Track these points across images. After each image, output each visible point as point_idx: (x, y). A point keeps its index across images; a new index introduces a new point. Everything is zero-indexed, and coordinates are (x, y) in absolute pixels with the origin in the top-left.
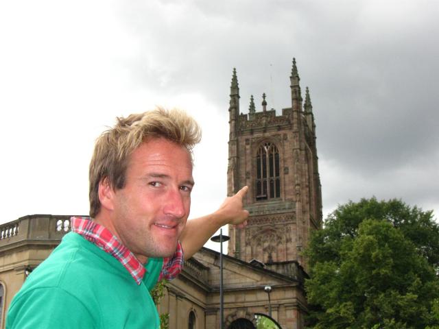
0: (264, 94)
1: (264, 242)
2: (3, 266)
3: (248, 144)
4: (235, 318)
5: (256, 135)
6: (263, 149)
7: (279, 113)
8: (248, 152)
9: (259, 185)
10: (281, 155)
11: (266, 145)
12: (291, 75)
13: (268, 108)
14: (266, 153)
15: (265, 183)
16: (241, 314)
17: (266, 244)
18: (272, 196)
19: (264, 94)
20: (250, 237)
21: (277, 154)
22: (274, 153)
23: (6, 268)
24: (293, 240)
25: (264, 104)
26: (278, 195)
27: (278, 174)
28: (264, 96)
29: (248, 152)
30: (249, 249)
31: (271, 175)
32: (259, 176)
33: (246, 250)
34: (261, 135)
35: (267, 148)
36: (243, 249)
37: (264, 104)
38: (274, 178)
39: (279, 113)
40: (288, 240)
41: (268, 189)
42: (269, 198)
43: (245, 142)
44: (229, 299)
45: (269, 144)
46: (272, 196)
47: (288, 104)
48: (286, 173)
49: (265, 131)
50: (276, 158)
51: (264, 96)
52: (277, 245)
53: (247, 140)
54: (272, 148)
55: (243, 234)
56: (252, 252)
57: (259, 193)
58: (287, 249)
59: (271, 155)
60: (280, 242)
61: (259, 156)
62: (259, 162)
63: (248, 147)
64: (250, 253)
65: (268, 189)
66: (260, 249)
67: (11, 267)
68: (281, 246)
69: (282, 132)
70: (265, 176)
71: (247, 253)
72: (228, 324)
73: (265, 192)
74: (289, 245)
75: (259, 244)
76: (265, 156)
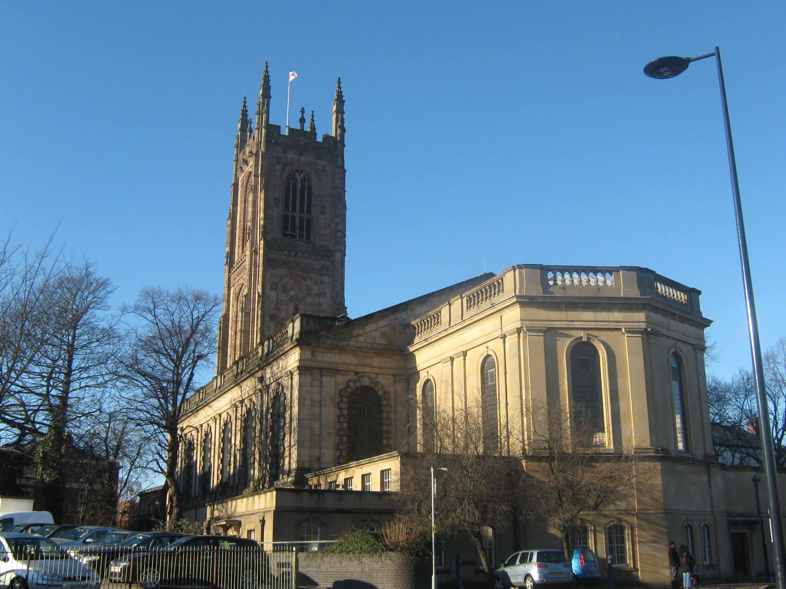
0: (303, 109)
5: (289, 156)
8: (278, 173)
9: (286, 218)
10: (314, 189)
14: (296, 180)
17: (292, 293)
18: (301, 236)
19: (303, 109)
21: (310, 187)
22: (306, 184)
23: (600, 325)
24: (328, 295)
26: (308, 237)
27: (309, 211)
28: (303, 111)
31: (302, 210)
32: (287, 207)
34: (296, 157)
38: (305, 216)
40: (321, 294)
42: (298, 238)
43: (275, 160)
45: (301, 172)
48: (323, 213)
49: (301, 155)
50: (308, 191)
51: (303, 111)
57: (285, 228)
58: (320, 305)
59: (303, 186)
60: (309, 295)
62: (287, 189)
63: (278, 167)
64: (275, 300)
66: (283, 297)
68: (309, 299)
69: (321, 162)
70: (294, 210)
71: (272, 299)
73: (293, 229)
74: (322, 300)
76: (295, 185)
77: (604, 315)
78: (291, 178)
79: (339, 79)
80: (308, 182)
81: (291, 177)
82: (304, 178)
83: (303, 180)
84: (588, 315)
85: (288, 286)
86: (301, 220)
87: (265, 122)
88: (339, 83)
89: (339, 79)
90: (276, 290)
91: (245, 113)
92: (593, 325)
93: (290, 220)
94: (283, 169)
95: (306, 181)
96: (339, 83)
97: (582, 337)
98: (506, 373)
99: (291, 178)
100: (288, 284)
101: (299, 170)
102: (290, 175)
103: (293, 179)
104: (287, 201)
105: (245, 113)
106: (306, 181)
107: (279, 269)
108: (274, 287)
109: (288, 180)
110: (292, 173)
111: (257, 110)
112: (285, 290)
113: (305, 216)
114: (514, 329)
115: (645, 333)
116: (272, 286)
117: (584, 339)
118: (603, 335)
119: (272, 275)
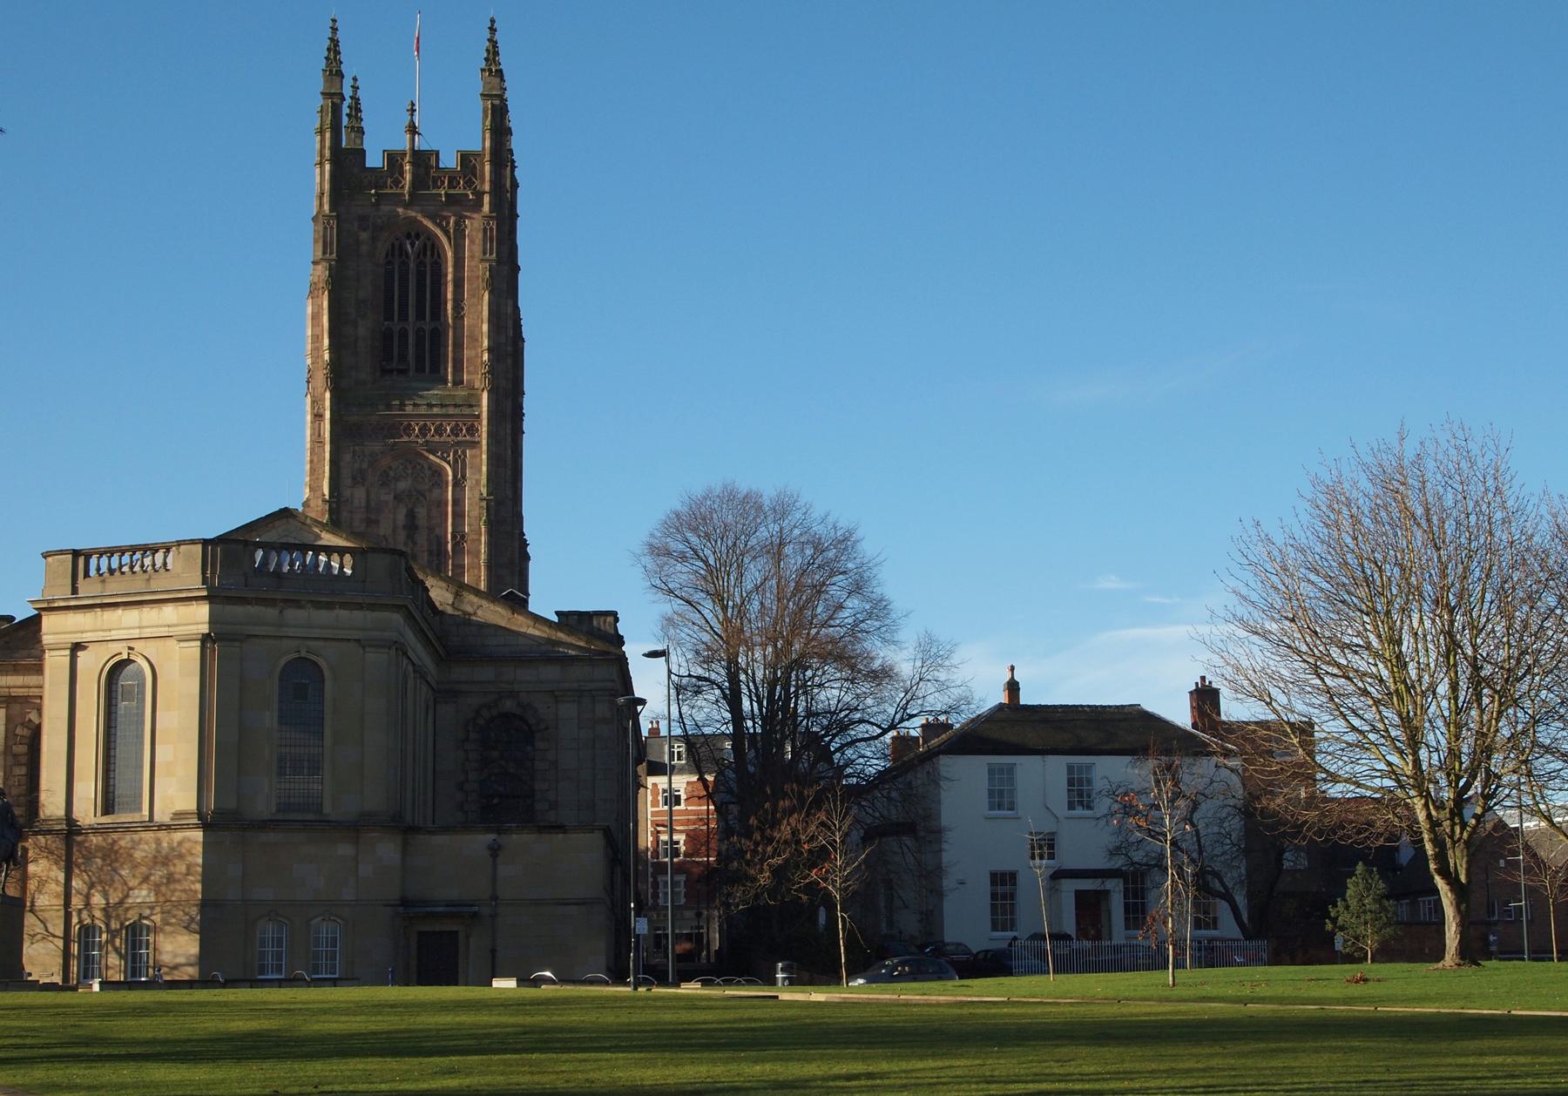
1: (397, 479)
3: (365, 230)
4: (495, 712)
6: (402, 247)
7: (449, 161)
9: (387, 336)
11: (408, 236)
12: (483, 64)
13: (421, 144)
15: (403, 335)
16: (508, 705)
17: (403, 485)
18: (420, 368)
20: (365, 465)
22: (428, 260)
23: (147, 633)
25: (413, 130)
29: (364, 249)
30: (359, 495)
31: (420, 315)
32: (389, 317)
33: (352, 495)
35: (412, 245)
36: (347, 493)
37: (413, 130)
39: (449, 161)
41: (411, 350)
42: (411, 373)
43: (356, 224)
44: (486, 673)
45: (418, 236)
46: (420, 368)
47: (476, 139)
52: (430, 490)
53: (363, 219)
54: (425, 245)
55: (347, 457)
56: (368, 501)
59: (421, 264)
61: (389, 263)
63: (364, 236)
64: (363, 504)
65: (411, 350)
67: (163, 631)
70: (404, 316)
72: (481, 722)
73: (403, 357)
75: (384, 484)
76: (404, 264)
77: (150, 615)
78: (397, 253)
79: (493, 21)
80: (432, 255)
81: (397, 251)
84: (130, 617)
85: (392, 474)
86: (419, 334)
87: (331, 148)
88: (493, 30)
89: (493, 21)
90: (363, 485)
92: (136, 633)
93: (396, 339)
94: (374, 239)
95: (429, 253)
97: (121, 653)
99: (397, 253)
100: (390, 468)
101: (413, 234)
102: (393, 245)
103: (401, 255)
104: (389, 300)
106: (429, 253)
107: (366, 443)
108: (359, 478)
109: (390, 257)
110: (397, 243)
111: (318, 125)
112: (385, 480)
113: (427, 326)
114: (68, 643)
115: (205, 639)
116: (354, 478)
117: (125, 656)
118: (150, 649)
119: (354, 456)
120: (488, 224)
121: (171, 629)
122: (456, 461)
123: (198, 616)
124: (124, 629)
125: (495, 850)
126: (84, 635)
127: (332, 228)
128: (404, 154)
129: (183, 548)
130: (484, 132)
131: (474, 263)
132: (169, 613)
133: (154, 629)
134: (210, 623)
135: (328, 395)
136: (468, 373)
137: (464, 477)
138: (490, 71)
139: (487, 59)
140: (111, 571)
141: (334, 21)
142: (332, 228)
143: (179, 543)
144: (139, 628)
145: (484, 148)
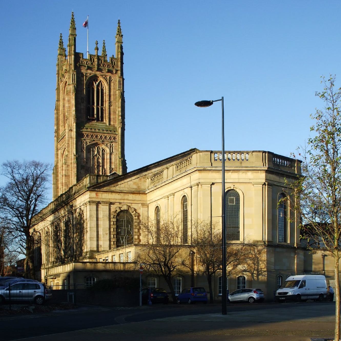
2: (238, 179)
23: (241, 181)
26: (102, 120)
27: (102, 105)
31: (98, 104)
35: (96, 84)
79: (119, 21)
82: (99, 84)
83: (98, 86)
88: (119, 23)
89: (119, 21)
91: (61, 43)
92: (237, 181)
96: (119, 23)
97: (231, 187)
98: (191, 205)
105: (61, 43)
111: (68, 43)
117: (232, 188)
120: (120, 79)
121: (250, 180)
122: (110, 147)
123: (262, 177)
124: (231, 179)
125: (324, 256)
126: (216, 180)
127: (75, 75)
128: (95, 56)
129: (254, 153)
130: (118, 53)
131: (115, 91)
132: (250, 175)
133: (244, 180)
134: (266, 179)
135: (75, 124)
136: (113, 122)
137: (112, 152)
138: (120, 35)
139: (118, 32)
140: (229, 159)
141: (73, 13)
142: (75, 75)
143: (253, 152)
144: (238, 179)
145: (118, 57)
